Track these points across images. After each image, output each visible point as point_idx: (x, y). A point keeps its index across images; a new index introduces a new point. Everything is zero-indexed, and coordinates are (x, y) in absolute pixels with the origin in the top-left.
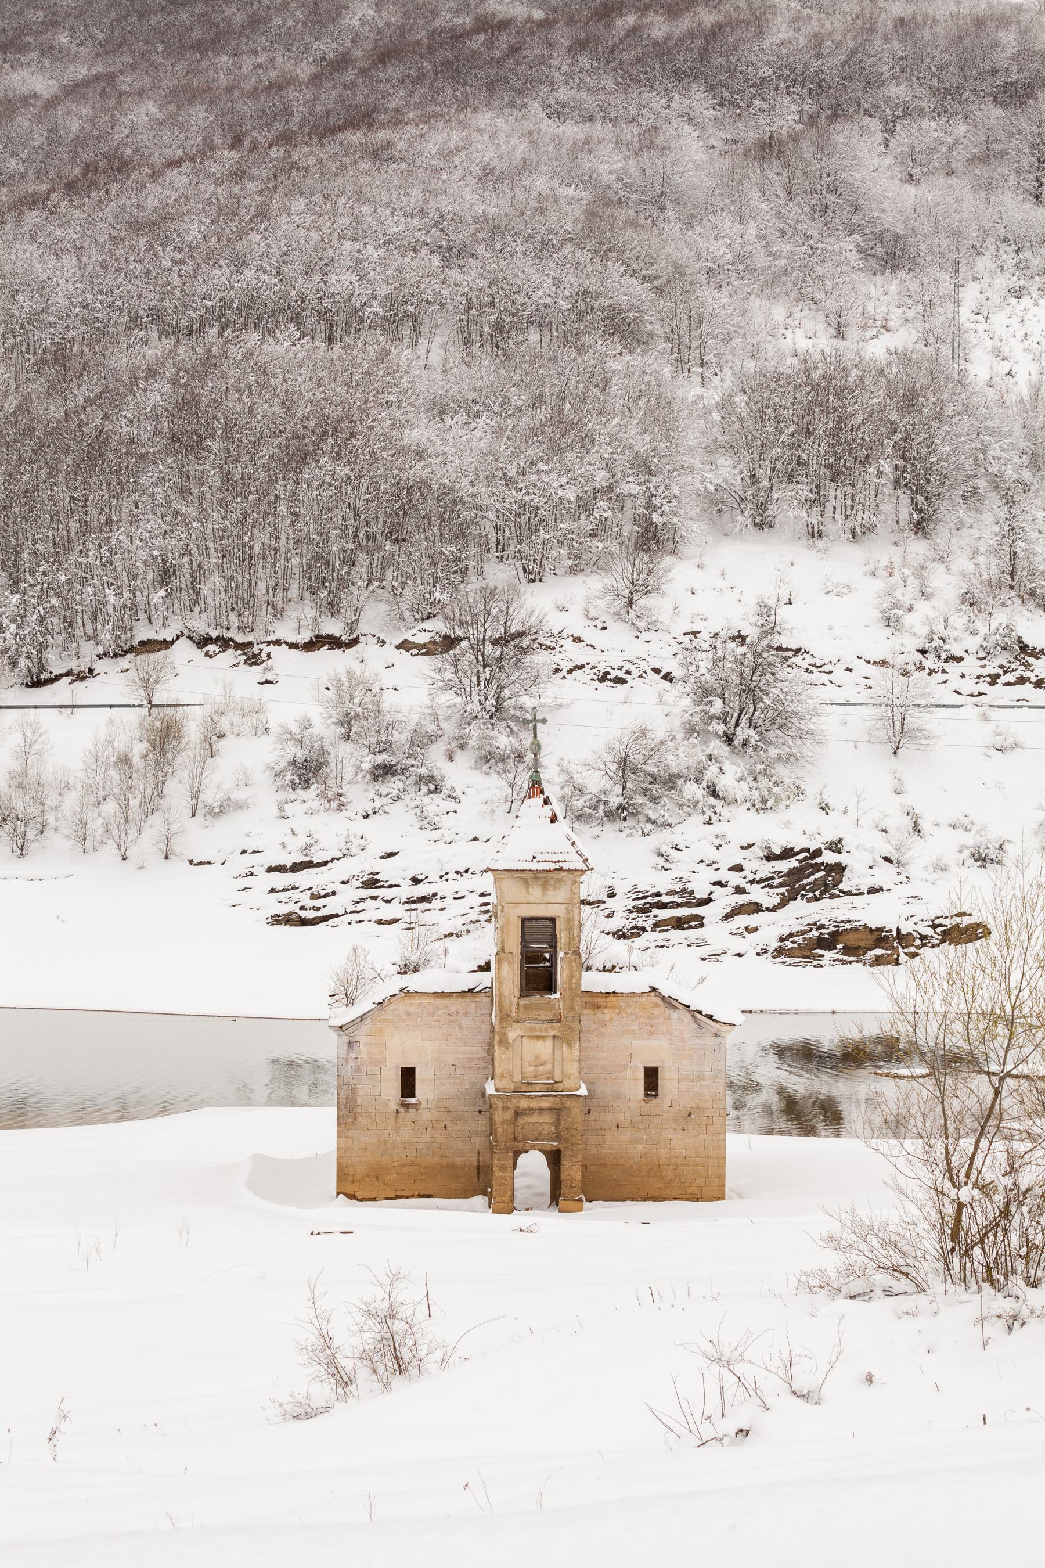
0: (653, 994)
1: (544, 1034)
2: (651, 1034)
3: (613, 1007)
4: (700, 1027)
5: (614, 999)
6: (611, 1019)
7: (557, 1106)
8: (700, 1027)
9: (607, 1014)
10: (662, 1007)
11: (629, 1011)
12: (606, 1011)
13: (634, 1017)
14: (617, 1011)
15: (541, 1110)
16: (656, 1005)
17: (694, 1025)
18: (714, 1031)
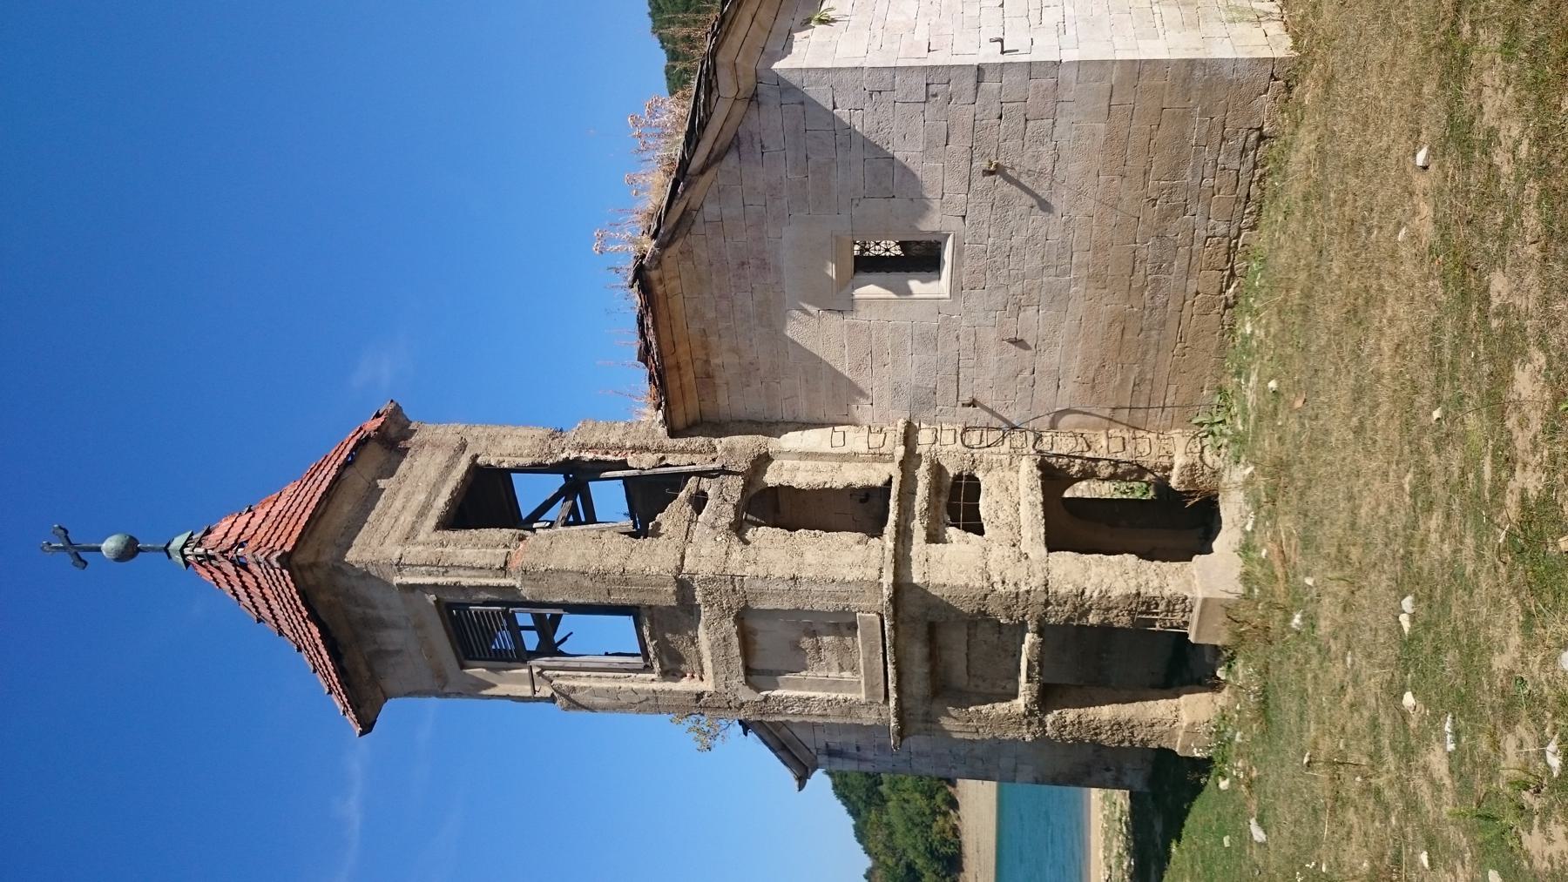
0: (654, 275)
1: (735, 640)
2: (763, 266)
3: (705, 346)
4: (735, 144)
5: (682, 349)
6: (735, 351)
7: (922, 630)
8: (735, 144)
9: (722, 359)
10: (692, 240)
11: (711, 315)
12: (715, 361)
13: (724, 305)
14: (713, 339)
15: (933, 657)
16: (687, 253)
17: (731, 160)
18: (740, 108)
